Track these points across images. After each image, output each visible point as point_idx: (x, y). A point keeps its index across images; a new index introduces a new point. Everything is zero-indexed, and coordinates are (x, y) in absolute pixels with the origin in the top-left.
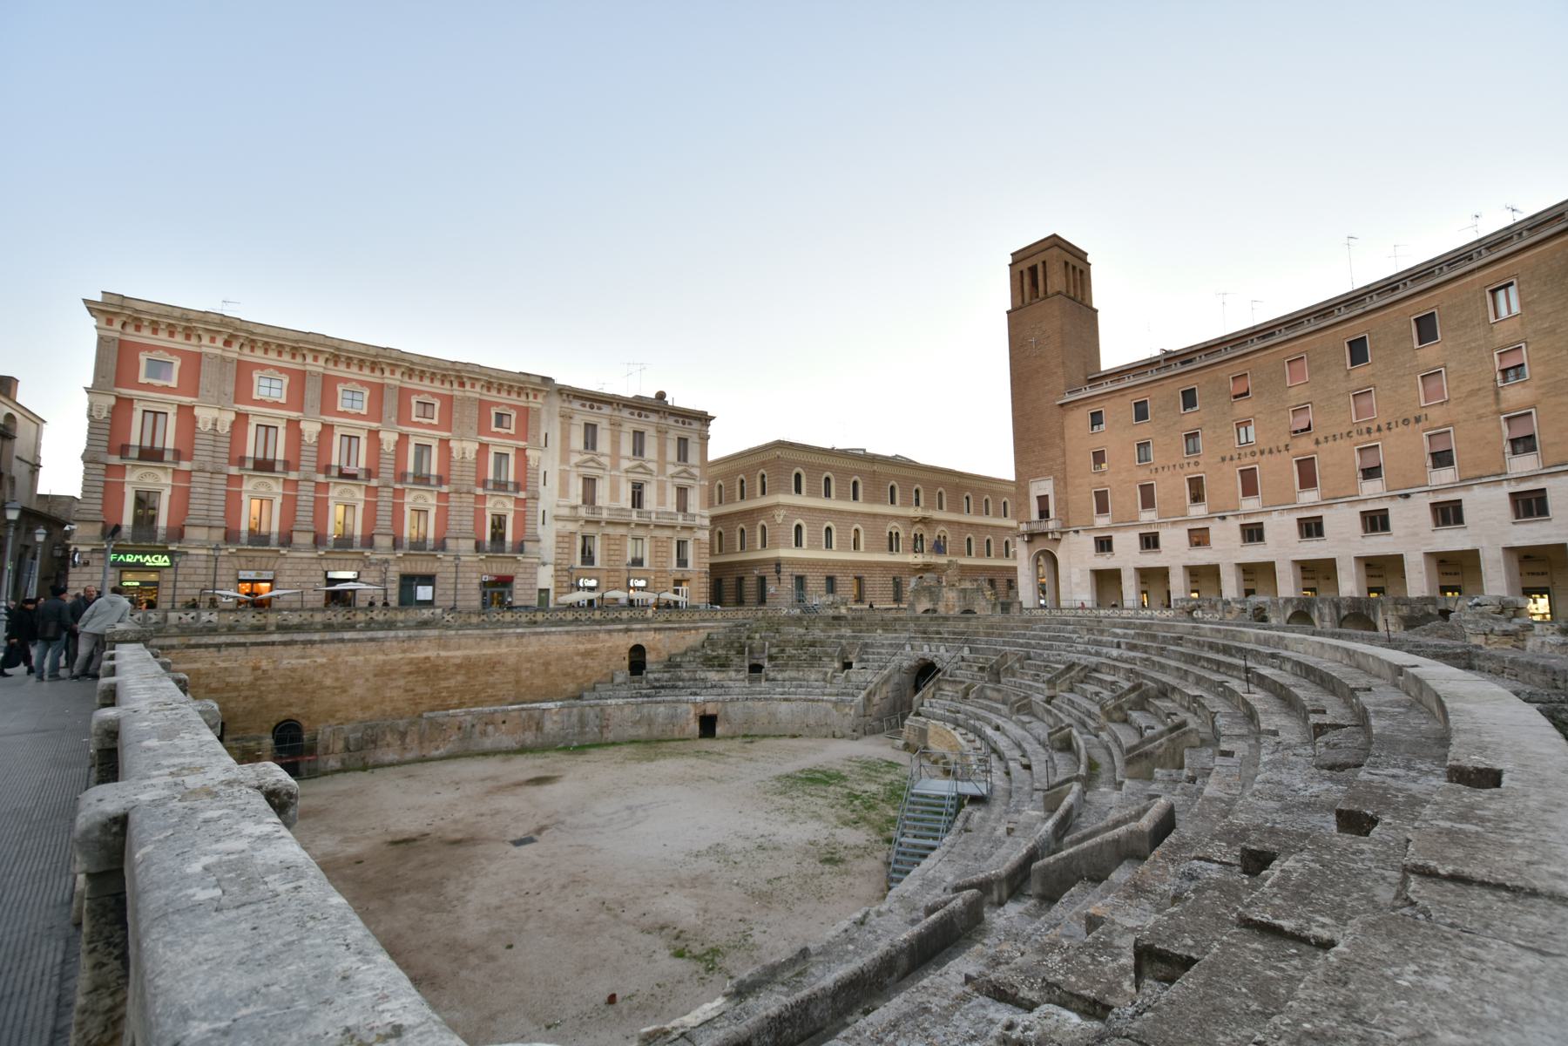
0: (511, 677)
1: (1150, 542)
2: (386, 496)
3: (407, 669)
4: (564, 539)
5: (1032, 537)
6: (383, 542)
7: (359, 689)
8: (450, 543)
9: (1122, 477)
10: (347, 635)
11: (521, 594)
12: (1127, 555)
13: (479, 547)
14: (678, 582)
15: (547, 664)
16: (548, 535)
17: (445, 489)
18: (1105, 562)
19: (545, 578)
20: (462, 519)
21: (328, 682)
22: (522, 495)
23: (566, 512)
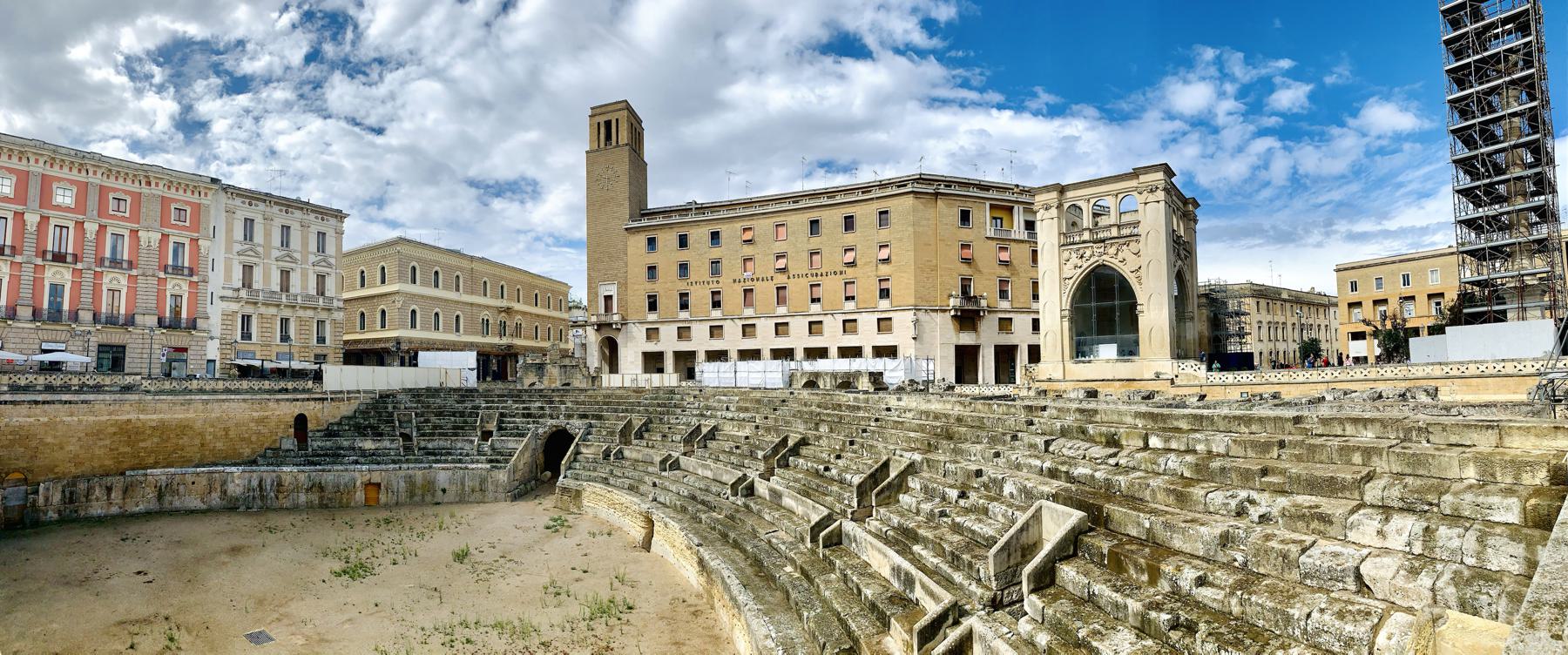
0: (197, 441)
1: (683, 333)
2: (88, 276)
3: (113, 430)
4: (228, 316)
5: (600, 327)
6: (86, 316)
7: (72, 448)
8: (139, 319)
9: (669, 287)
10: (65, 397)
11: (194, 364)
12: (668, 343)
13: (161, 323)
14: (317, 356)
15: (227, 430)
16: (216, 316)
17: (134, 272)
18: (652, 347)
19: (213, 351)
20: (147, 299)
21: (49, 440)
22: (195, 279)
23: (230, 293)
